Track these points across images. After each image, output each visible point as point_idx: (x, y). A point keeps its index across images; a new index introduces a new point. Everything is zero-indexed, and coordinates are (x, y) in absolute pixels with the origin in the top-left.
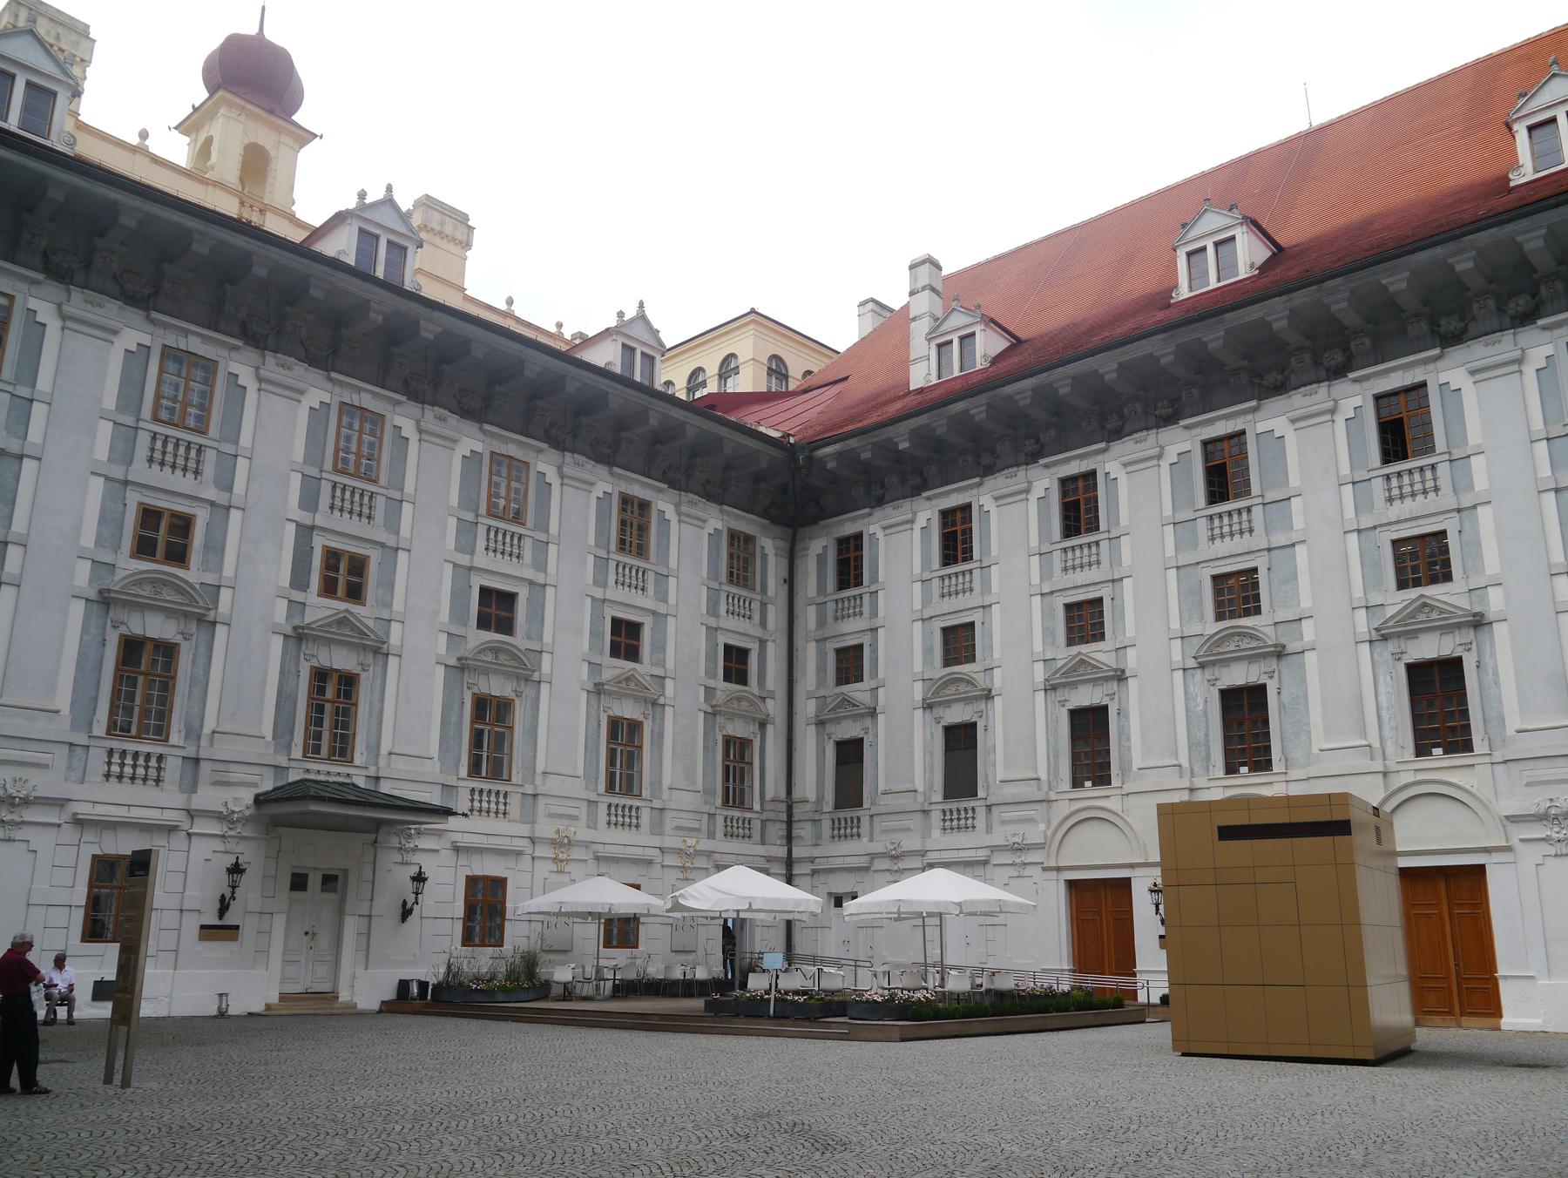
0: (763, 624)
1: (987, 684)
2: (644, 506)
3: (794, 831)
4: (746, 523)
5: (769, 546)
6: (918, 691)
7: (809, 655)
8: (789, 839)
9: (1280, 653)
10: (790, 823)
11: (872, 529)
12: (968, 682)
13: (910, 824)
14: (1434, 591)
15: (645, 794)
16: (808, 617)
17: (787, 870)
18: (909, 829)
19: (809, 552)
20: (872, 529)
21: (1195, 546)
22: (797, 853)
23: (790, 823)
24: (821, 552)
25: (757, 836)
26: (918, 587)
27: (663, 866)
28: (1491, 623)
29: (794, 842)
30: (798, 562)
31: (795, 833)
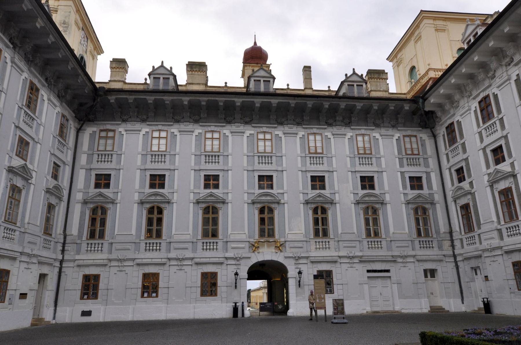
0: (66, 156)
1: (170, 198)
2: (38, 90)
3: (66, 248)
4: (68, 113)
5: (72, 126)
6: (136, 197)
7: (81, 176)
8: (63, 251)
9: (278, 203)
10: (64, 244)
11: (120, 130)
12: (161, 196)
13: (130, 247)
14: (322, 191)
15: (18, 224)
16: (83, 159)
17: (60, 265)
18: (129, 249)
19: (85, 132)
20: (120, 130)
22: (66, 257)
23: (64, 244)
24: (92, 133)
25: (52, 250)
26: (140, 156)
27: (20, 261)
28: (336, 203)
29: (65, 252)
30: (80, 134)
31: (66, 248)
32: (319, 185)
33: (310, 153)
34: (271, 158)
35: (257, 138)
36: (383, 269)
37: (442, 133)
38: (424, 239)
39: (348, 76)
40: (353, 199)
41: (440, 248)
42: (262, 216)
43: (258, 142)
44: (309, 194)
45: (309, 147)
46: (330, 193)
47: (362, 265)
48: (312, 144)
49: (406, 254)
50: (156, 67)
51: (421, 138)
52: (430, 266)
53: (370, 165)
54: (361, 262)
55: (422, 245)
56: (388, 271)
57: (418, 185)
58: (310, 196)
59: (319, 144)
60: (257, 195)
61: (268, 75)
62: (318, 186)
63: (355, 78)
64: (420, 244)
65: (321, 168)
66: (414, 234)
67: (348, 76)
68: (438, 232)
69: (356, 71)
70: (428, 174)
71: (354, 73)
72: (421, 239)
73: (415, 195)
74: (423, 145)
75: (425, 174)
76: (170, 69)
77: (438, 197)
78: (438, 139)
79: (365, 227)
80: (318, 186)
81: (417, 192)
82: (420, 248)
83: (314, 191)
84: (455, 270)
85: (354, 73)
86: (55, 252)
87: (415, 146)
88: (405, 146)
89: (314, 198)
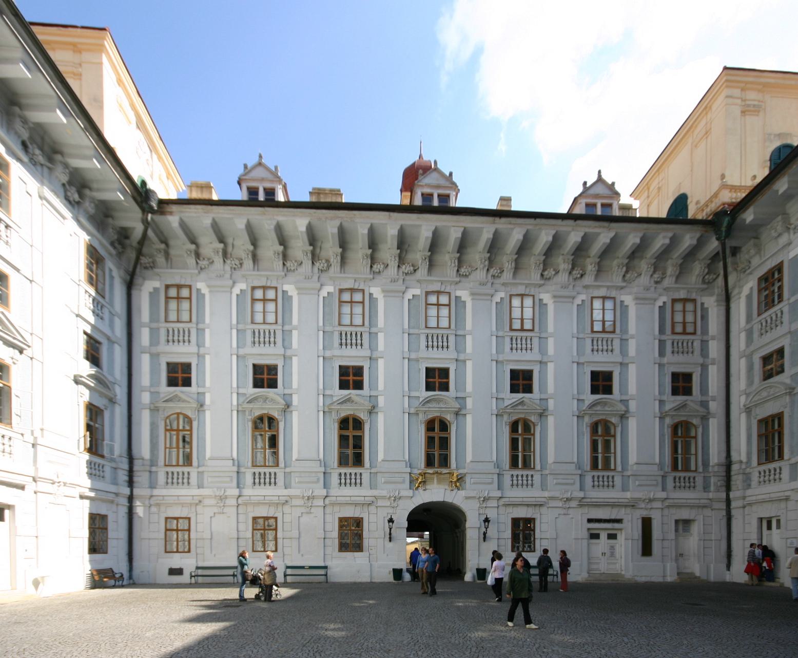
21: (418, 350)
32: (523, 385)
33: (511, 330)
34: (447, 339)
35: (426, 301)
36: (613, 517)
37: (746, 291)
38: (682, 474)
39: (588, 185)
40: (575, 409)
41: (706, 488)
42: (431, 434)
43: (426, 309)
44: (505, 400)
45: (511, 319)
46: (540, 399)
47: (580, 511)
48: (516, 313)
49: (652, 497)
50: (249, 166)
51: (702, 304)
52: (685, 514)
53: (610, 353)
54: (581, 506)
55: (678, 484)
56: (619, 521)
57: (684, 388)
58: (507, 403)
59: (528, 313)
60: (423, 401)
61: (447, 184)
62: (521, 387)
63: (600, 190)
64: (675, 482)
65: (528, 356)
66: (668, 467)
67: (588, 185)
68: (706, 464)
69: (604, 176)
70: (704, 367)
71: (600, 180)
72: (678, 474)
73: (678, 403)
74: (704, 317)
75: (699, 369)
76: (274, 170)
77: (716, 407)
78: (733, 306)
79: (591, 454)
80: (521, 387)
81: (680, 399)
82: (675, 487)
83: (514, 395)
84: (724, 522)
85: (600, 180)
86: (115, 482)
87: (690, 318)
88: (672, 319)
89: (514, 406)
